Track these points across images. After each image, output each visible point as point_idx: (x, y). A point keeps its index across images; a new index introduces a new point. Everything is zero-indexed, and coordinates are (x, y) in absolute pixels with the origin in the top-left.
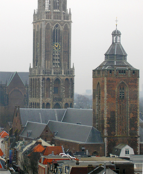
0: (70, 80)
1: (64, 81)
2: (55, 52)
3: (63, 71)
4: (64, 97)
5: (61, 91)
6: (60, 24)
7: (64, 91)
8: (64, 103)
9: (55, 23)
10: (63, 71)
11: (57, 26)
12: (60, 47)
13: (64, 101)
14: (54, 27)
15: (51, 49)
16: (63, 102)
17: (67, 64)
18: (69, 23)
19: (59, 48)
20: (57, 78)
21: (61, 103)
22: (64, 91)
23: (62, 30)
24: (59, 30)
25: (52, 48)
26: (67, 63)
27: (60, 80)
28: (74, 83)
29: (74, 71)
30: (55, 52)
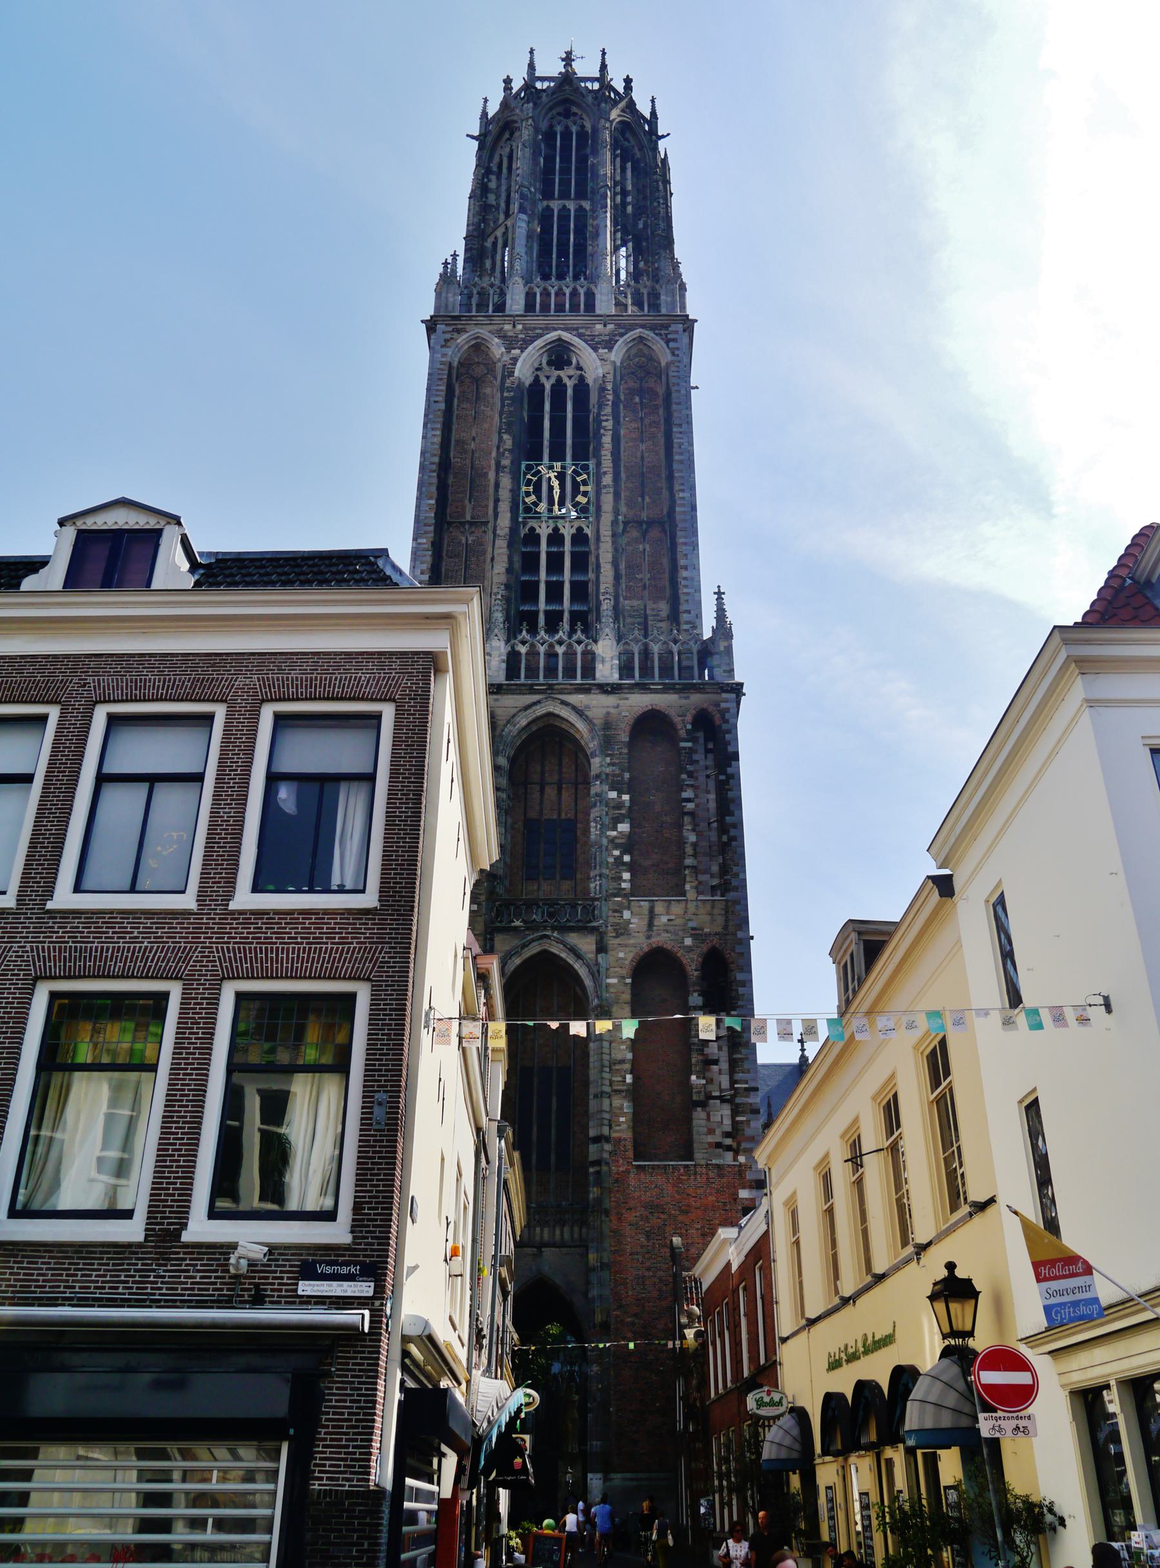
0: (684, 725)
1: (624, 737)
2: (544, 531)
3: (607, 650)
4: (619, 892)
5: (594, 831)
6: (580, 336)
7: (624, 827)
8: (623, 954)
9: (541, 336)
10: (607, 650)
11: (559, 355)
12: (582, 488)
13: (622, 930)
14: (537, 369)
15: (497, 501)
16: (612, 942)
17: (664, 613)
18: (667, 327)
19: (580, 499)
20: (540, 711)
21: (586, 944)
22: (624, 827)
23: (600, 372)
24: (582, 387)
25: (505, 494)
26: (664, 608)
27: (580, 725)
28: (735, 756)
29: (729, 651)
30: (544, 531)
